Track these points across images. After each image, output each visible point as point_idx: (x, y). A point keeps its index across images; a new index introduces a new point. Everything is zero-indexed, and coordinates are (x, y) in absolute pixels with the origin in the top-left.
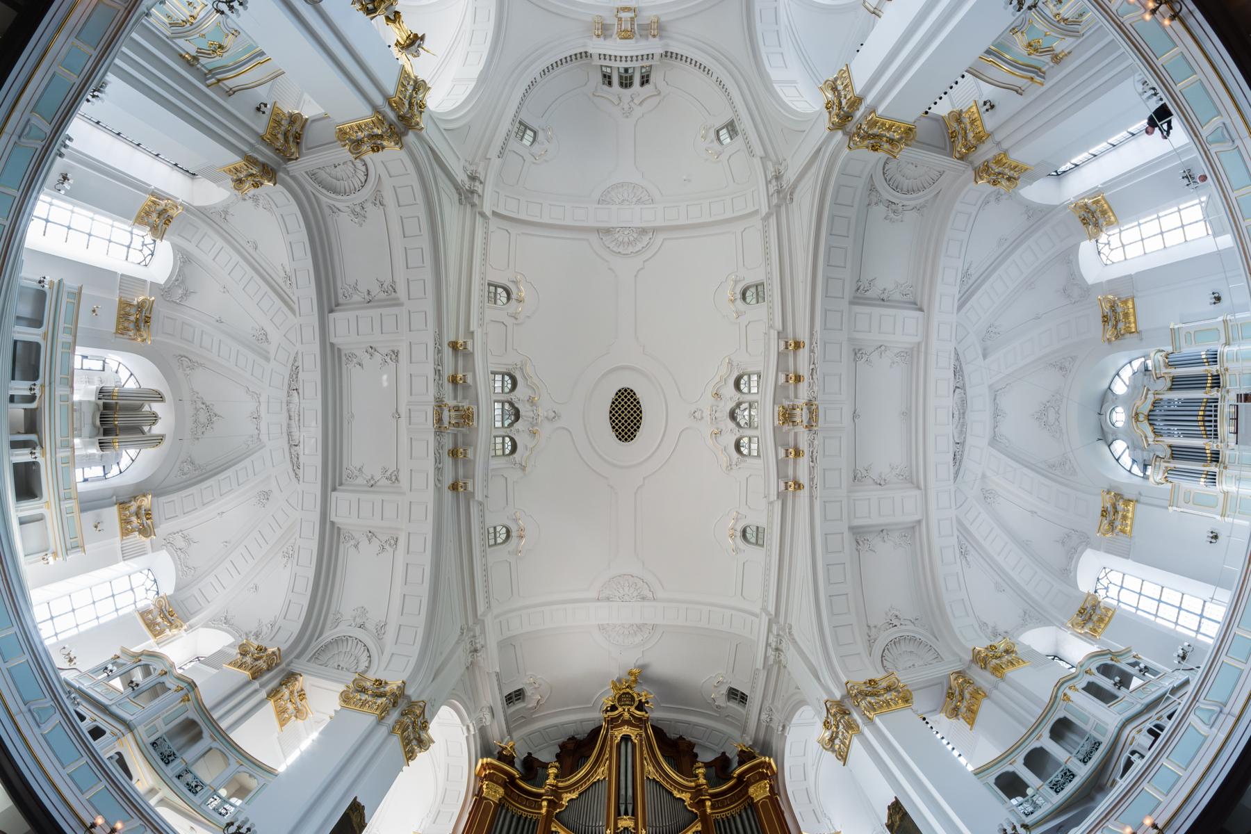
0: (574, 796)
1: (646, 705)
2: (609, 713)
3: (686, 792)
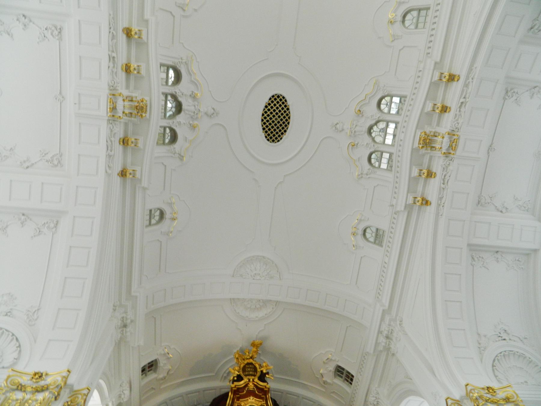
1: (267, 376)
2: (236, 383)
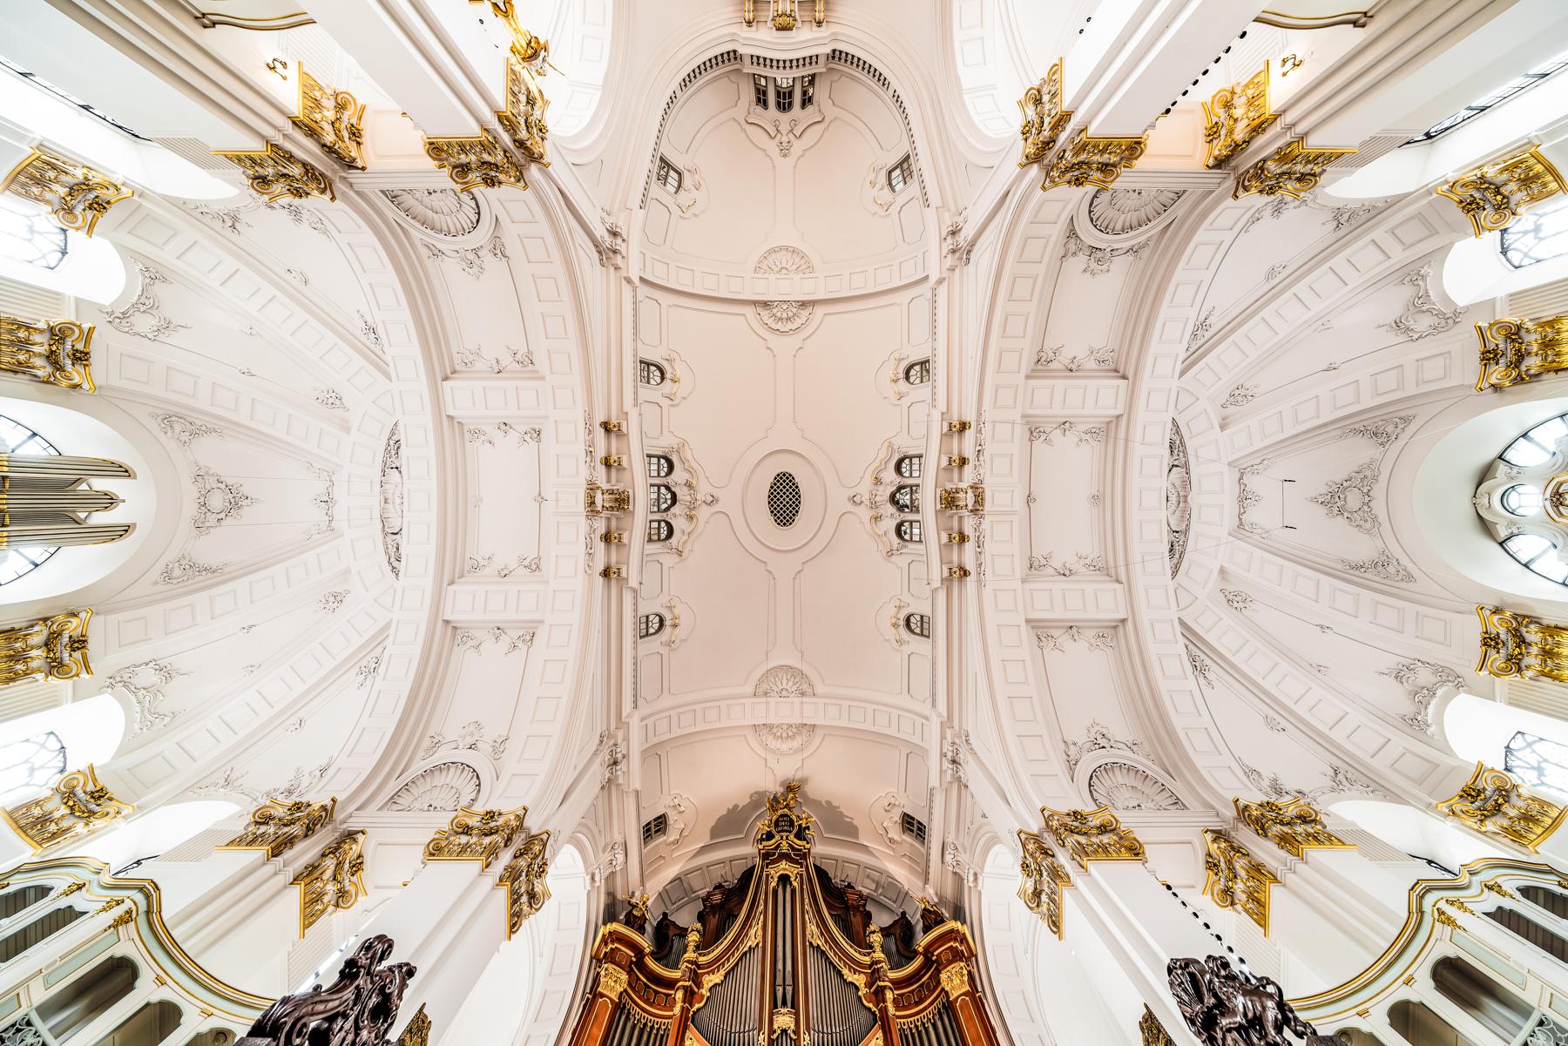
0: (717, 978)
2: (764, 843)
3: (860, 972)
